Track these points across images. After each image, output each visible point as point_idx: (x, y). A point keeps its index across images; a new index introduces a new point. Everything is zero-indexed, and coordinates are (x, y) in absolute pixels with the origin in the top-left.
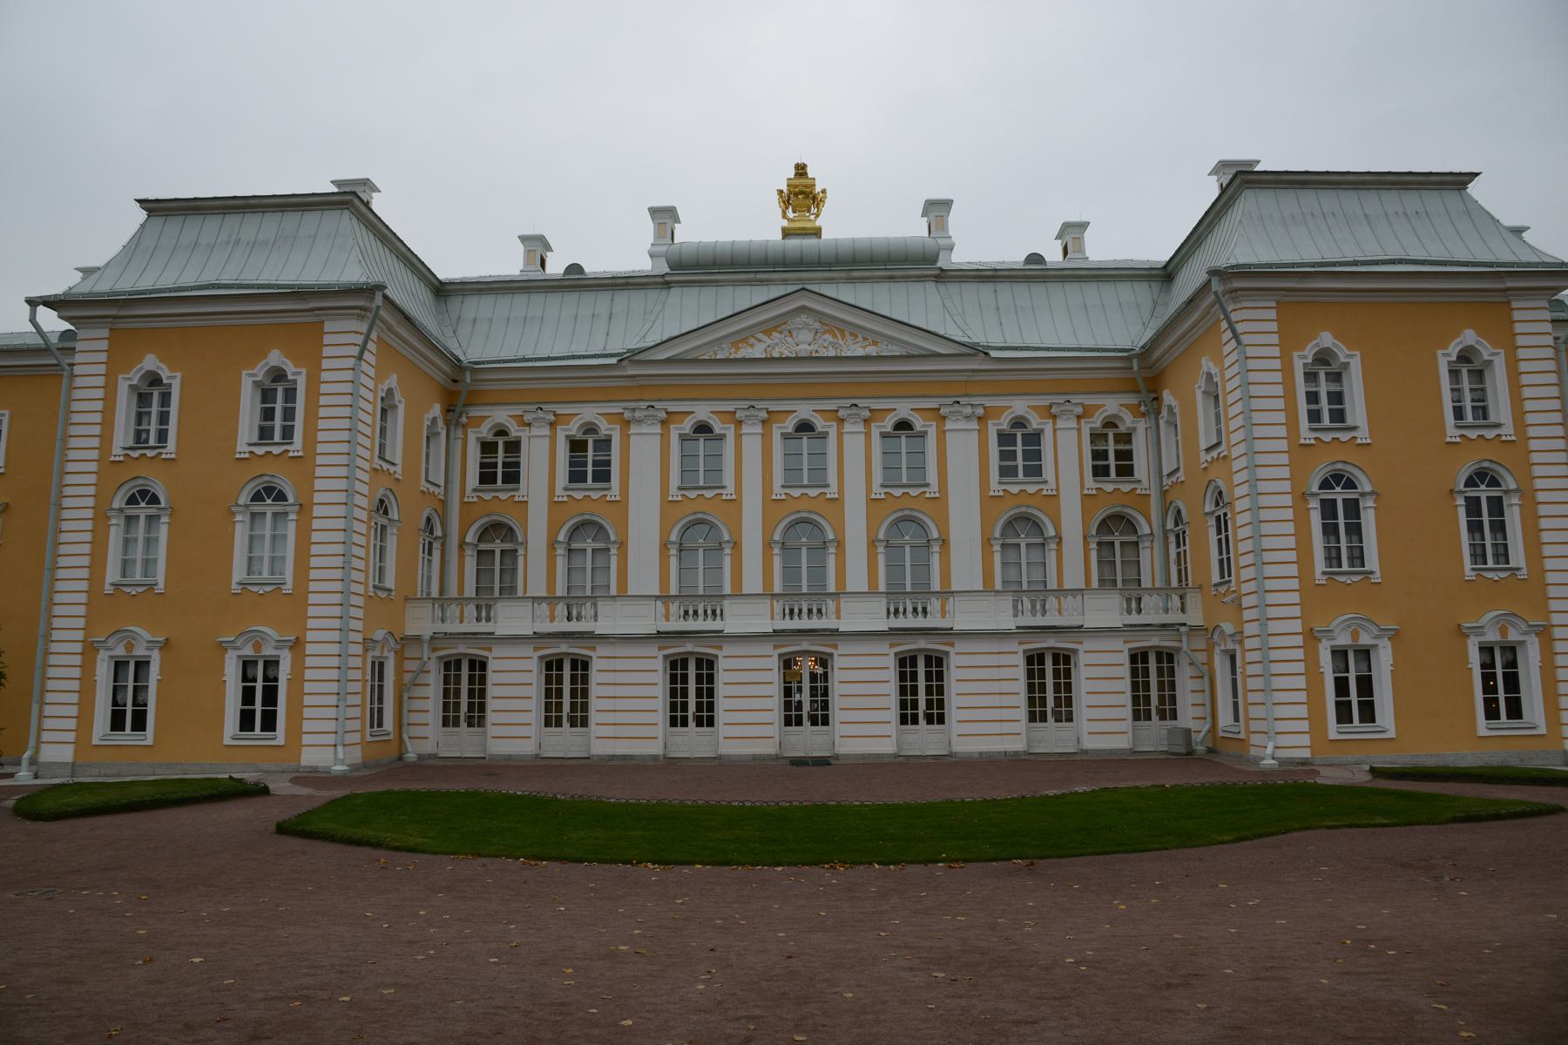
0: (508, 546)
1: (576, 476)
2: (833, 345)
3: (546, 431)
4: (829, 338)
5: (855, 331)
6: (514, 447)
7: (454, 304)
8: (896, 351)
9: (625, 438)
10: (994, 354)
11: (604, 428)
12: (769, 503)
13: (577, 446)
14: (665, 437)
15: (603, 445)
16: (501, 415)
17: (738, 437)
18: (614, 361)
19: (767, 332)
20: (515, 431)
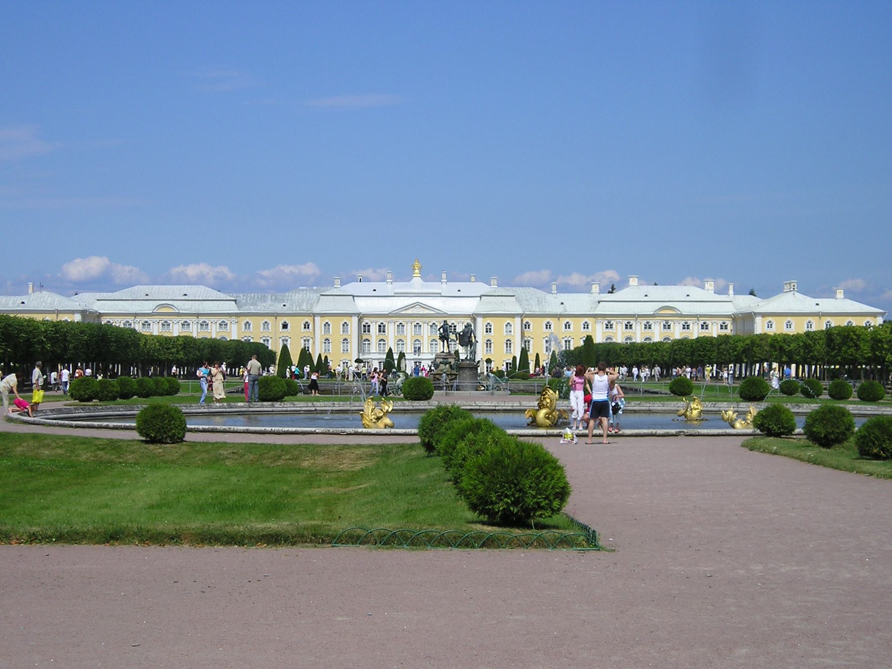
0: (369, 342)
1: (380, 331)
2: (423, 310)
3: (375, 324)
4: (422, 309)
5: (426, 308)
6: (369, 326)
7: (355, 298)
8: (433, 312)
9: (388, 325)
10: (449, 313)
11: (384, 323)
12: (412, 337)
13: (380, 326)
14: (395, 325)
15: (384, 326)
16: (367, 321)
17: (407, 326)
18: (387, 313)
19: (412, 308)
20: (370, 323)
